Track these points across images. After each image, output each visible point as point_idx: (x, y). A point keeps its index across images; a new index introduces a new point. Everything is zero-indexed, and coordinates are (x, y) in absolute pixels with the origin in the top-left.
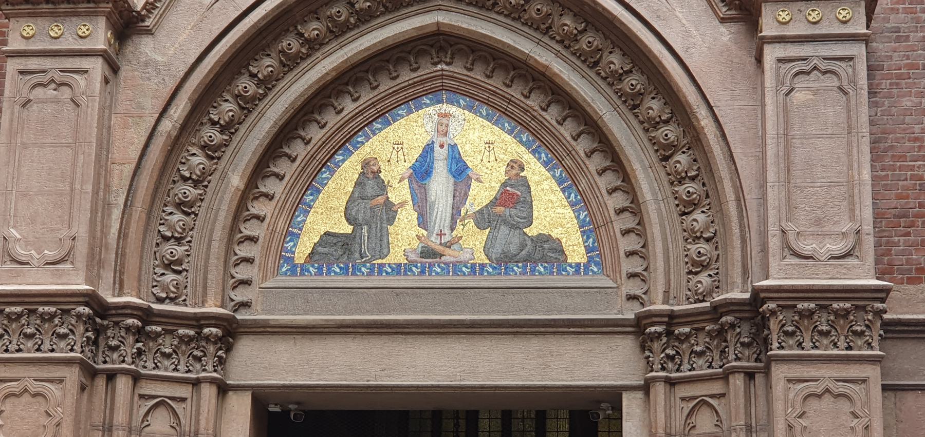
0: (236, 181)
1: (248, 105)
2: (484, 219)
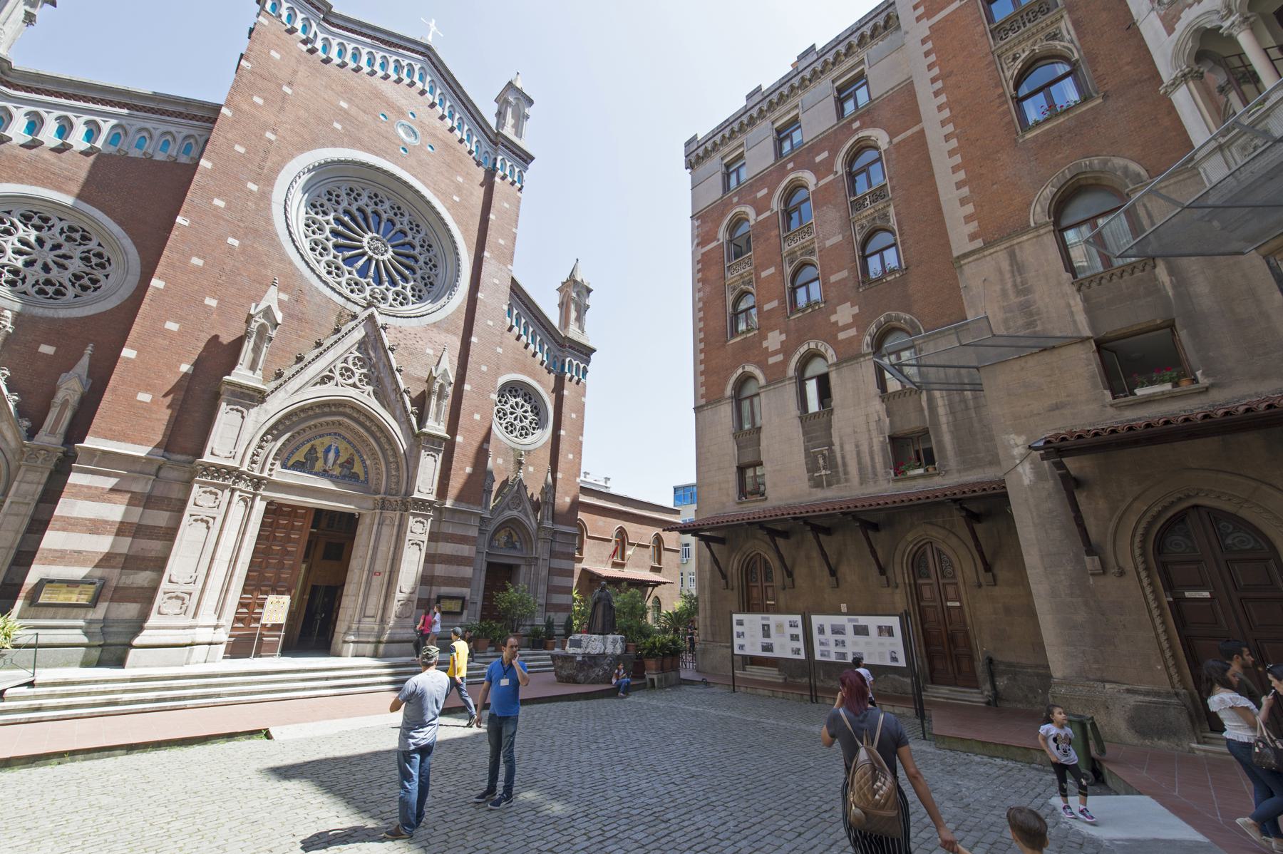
2: (341, 465)
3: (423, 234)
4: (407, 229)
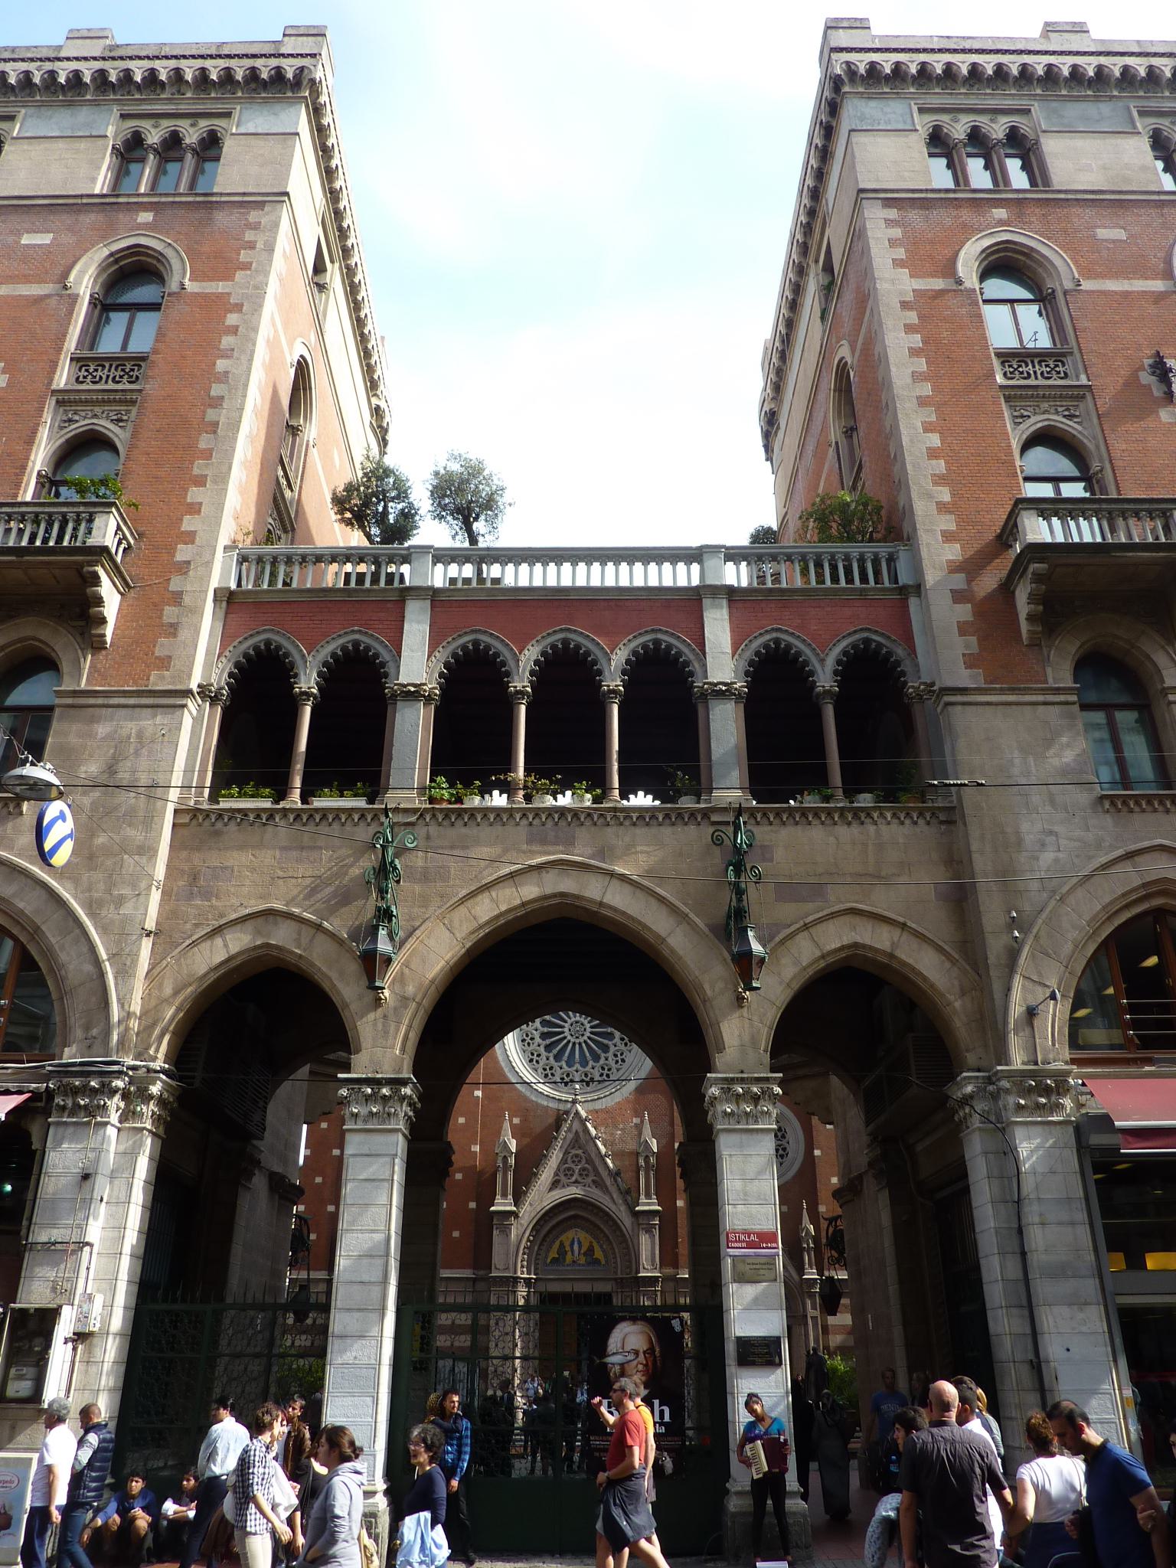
2: (585, 1254)
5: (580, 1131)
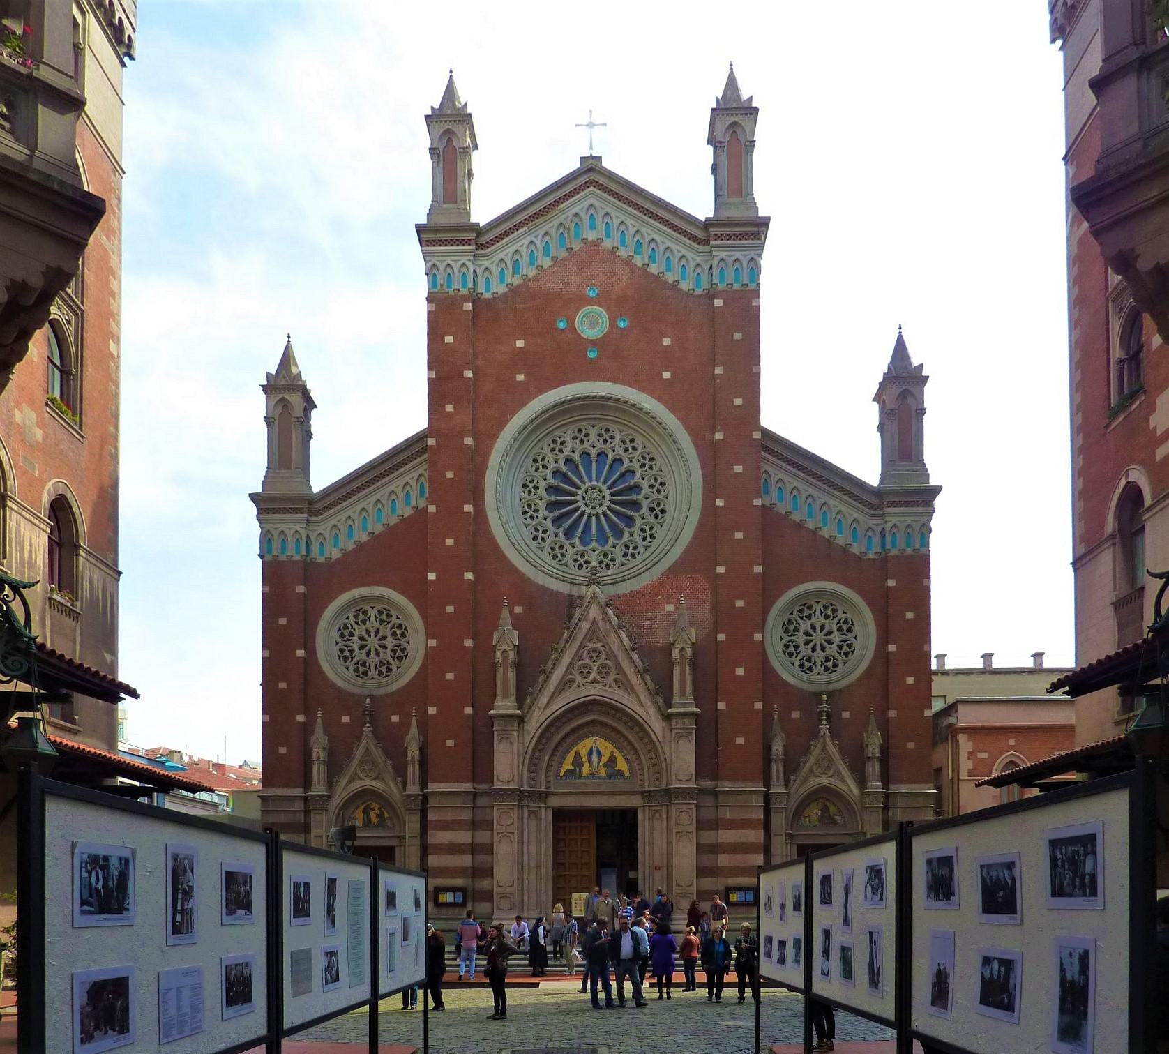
0: (547, 758)
1: (548, 739)
2: (605, 765)
3: (640, 449)
4: (620, 452)
5: (599, 619)
